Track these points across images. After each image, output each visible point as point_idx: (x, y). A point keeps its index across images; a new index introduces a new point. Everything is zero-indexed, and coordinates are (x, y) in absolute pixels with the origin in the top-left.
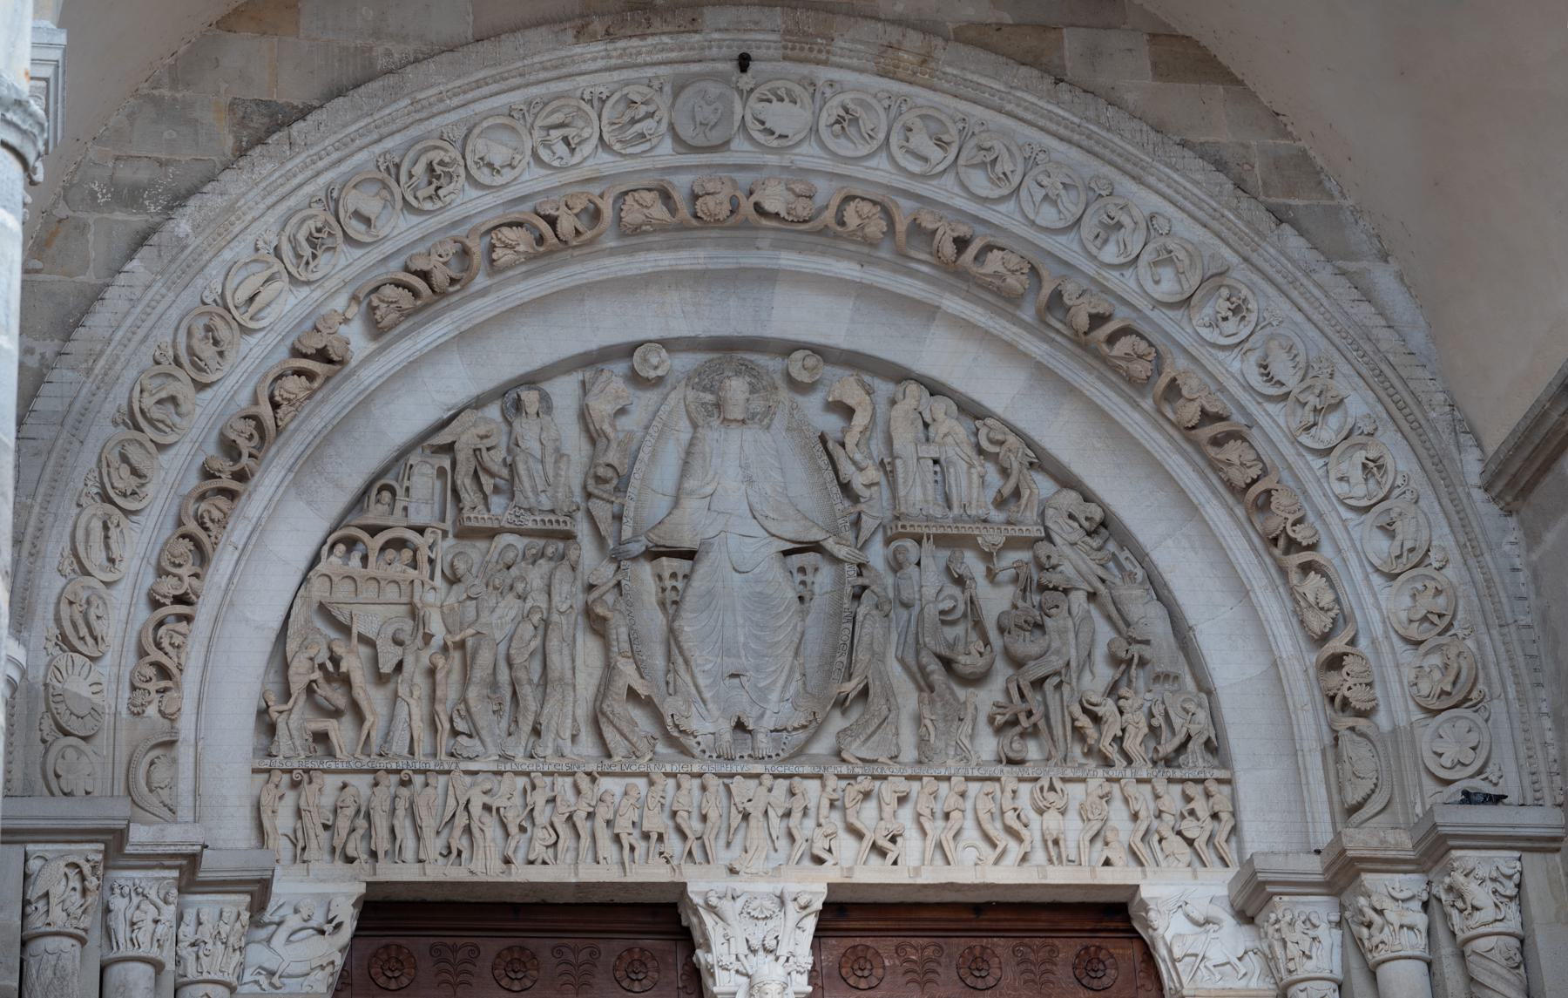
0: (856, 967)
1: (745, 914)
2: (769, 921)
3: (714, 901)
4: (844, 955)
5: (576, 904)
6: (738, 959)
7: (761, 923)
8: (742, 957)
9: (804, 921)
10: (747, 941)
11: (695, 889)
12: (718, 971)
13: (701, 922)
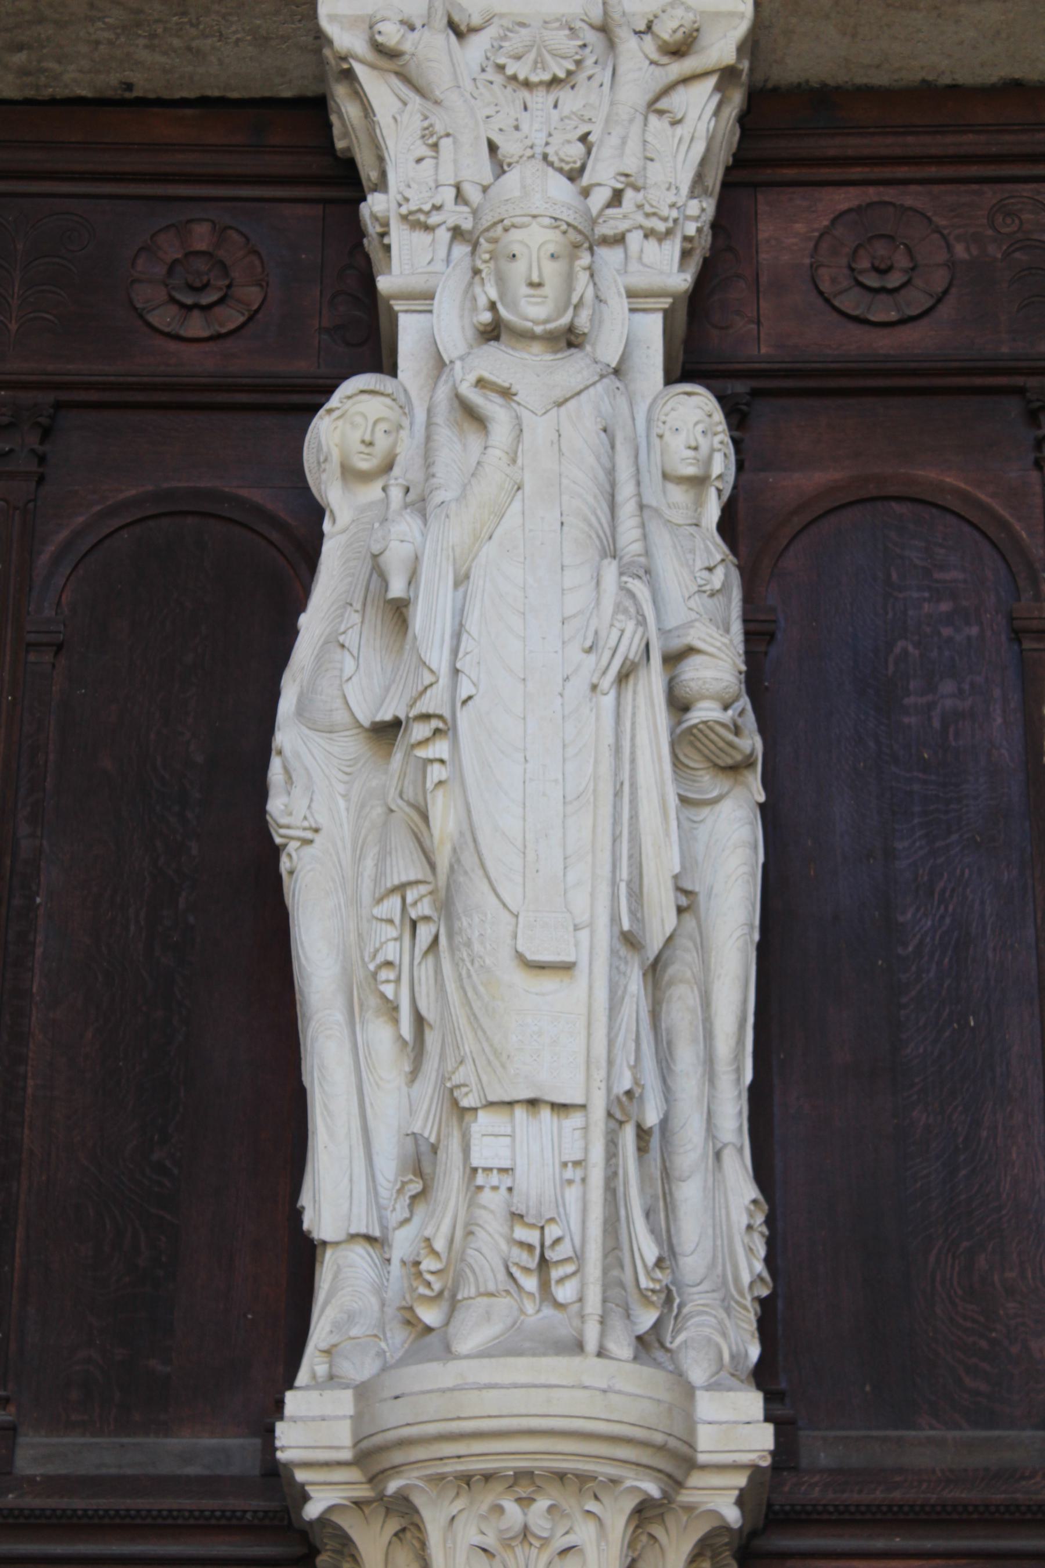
0: (864, 264)
1: (491, 74)
2: (564, 94)
3: (391, 34)
4: (824, 233)
5: (28, 102)
6: (460, 197)
7: (540, 99)
8: (473, 194)
9: (679, 100)
10: (492, 147)
11: (343, 9)
12: (399, 237)
13: (367, 110)
